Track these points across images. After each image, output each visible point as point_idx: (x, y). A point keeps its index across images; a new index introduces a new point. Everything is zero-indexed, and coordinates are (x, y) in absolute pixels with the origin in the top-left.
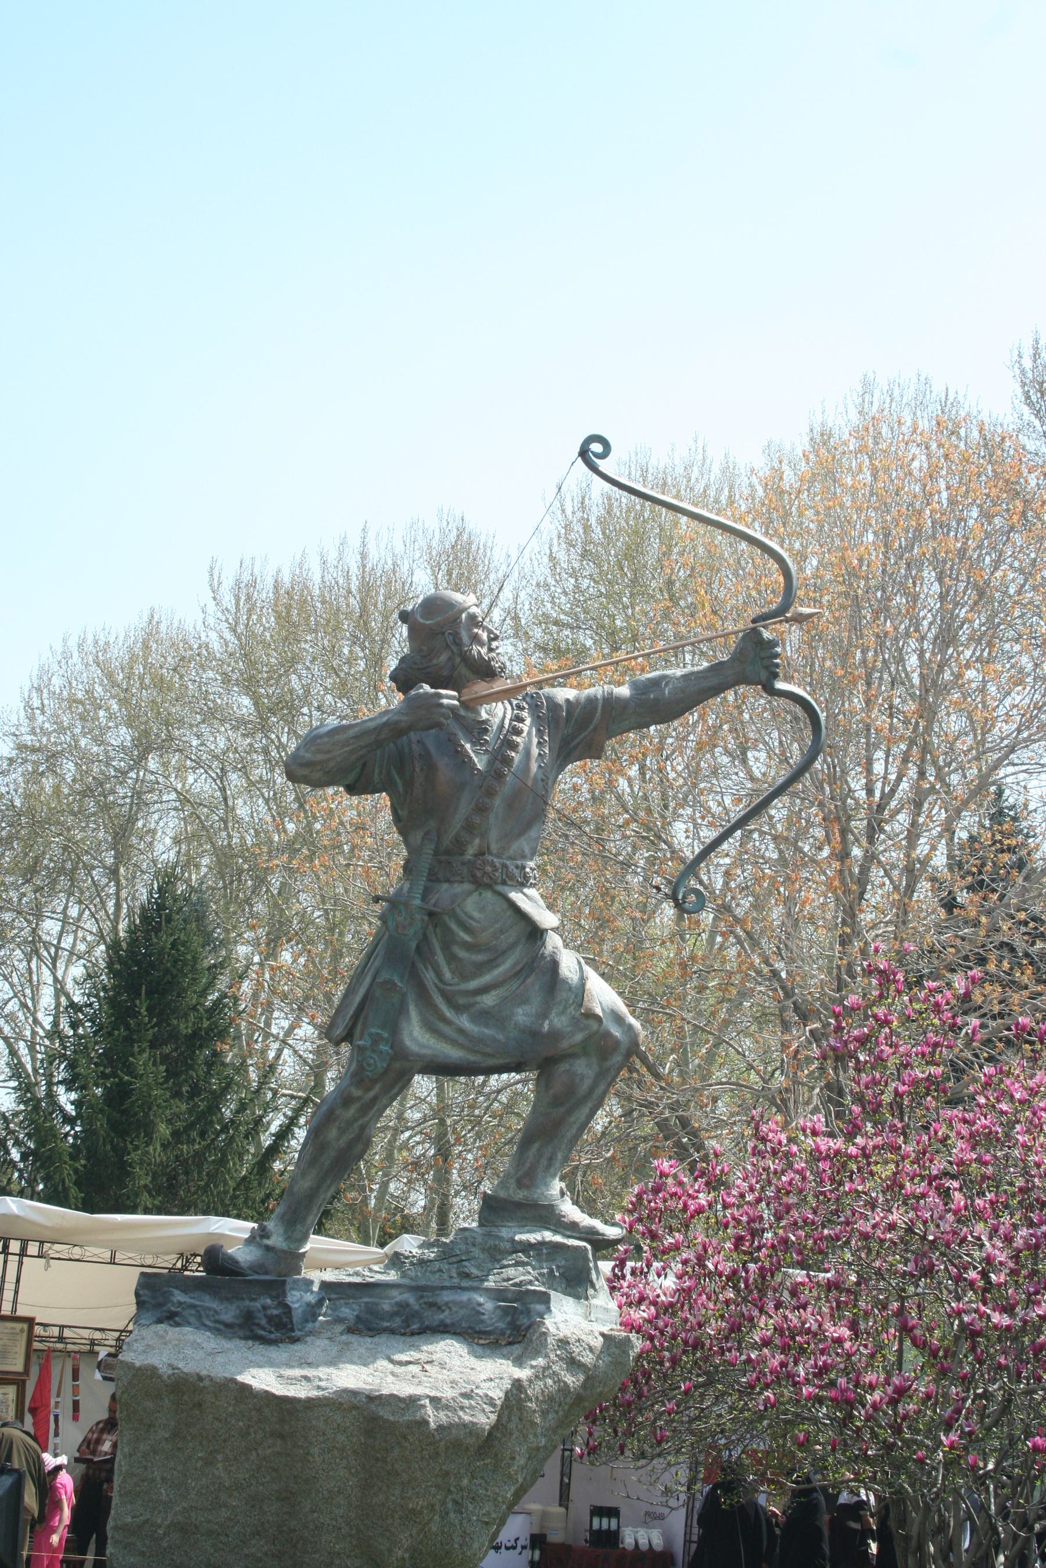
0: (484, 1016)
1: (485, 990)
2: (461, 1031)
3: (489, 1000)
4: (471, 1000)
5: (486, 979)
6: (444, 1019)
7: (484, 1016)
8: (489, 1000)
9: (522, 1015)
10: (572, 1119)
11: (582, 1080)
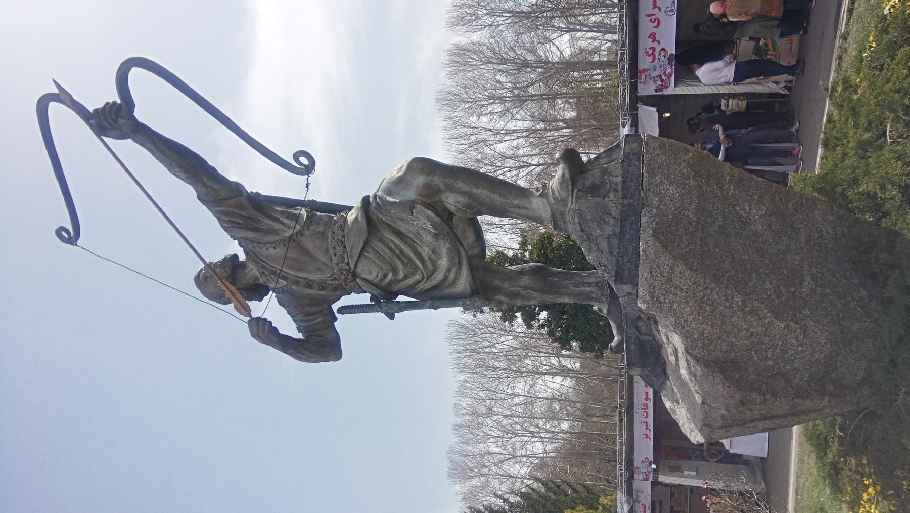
2: (449, 270)
3: (425, 251)
4: (428, 262)
6: (446, 278)
10: (488, 201)
11: (458, 202)
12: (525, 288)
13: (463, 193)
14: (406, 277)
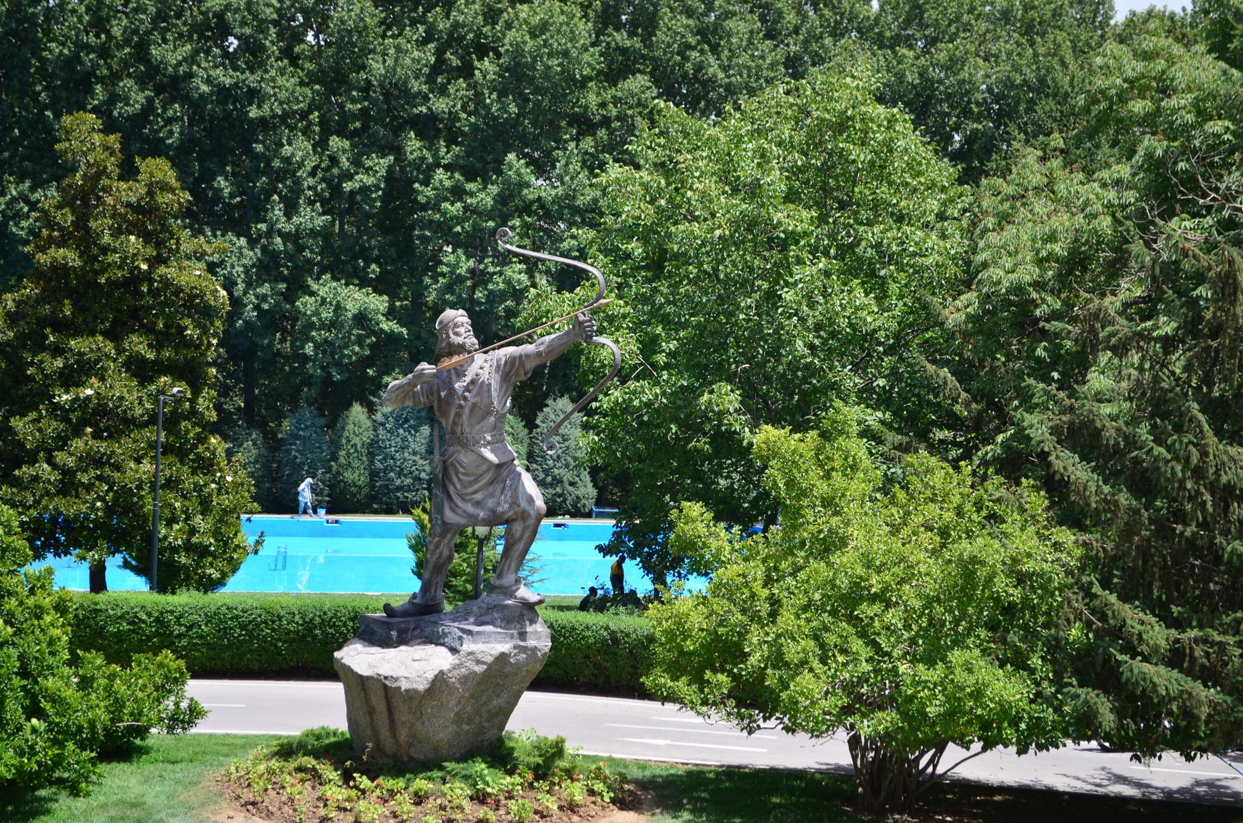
0: (478, 504)
1: (475, 492)
3: (478, 496)
5: (476, 487)
7: (478, 504)
8: (478, 496)
9: (490, 503)
12: (441, 553)
13: (522, 536)
14: (459, 480)
